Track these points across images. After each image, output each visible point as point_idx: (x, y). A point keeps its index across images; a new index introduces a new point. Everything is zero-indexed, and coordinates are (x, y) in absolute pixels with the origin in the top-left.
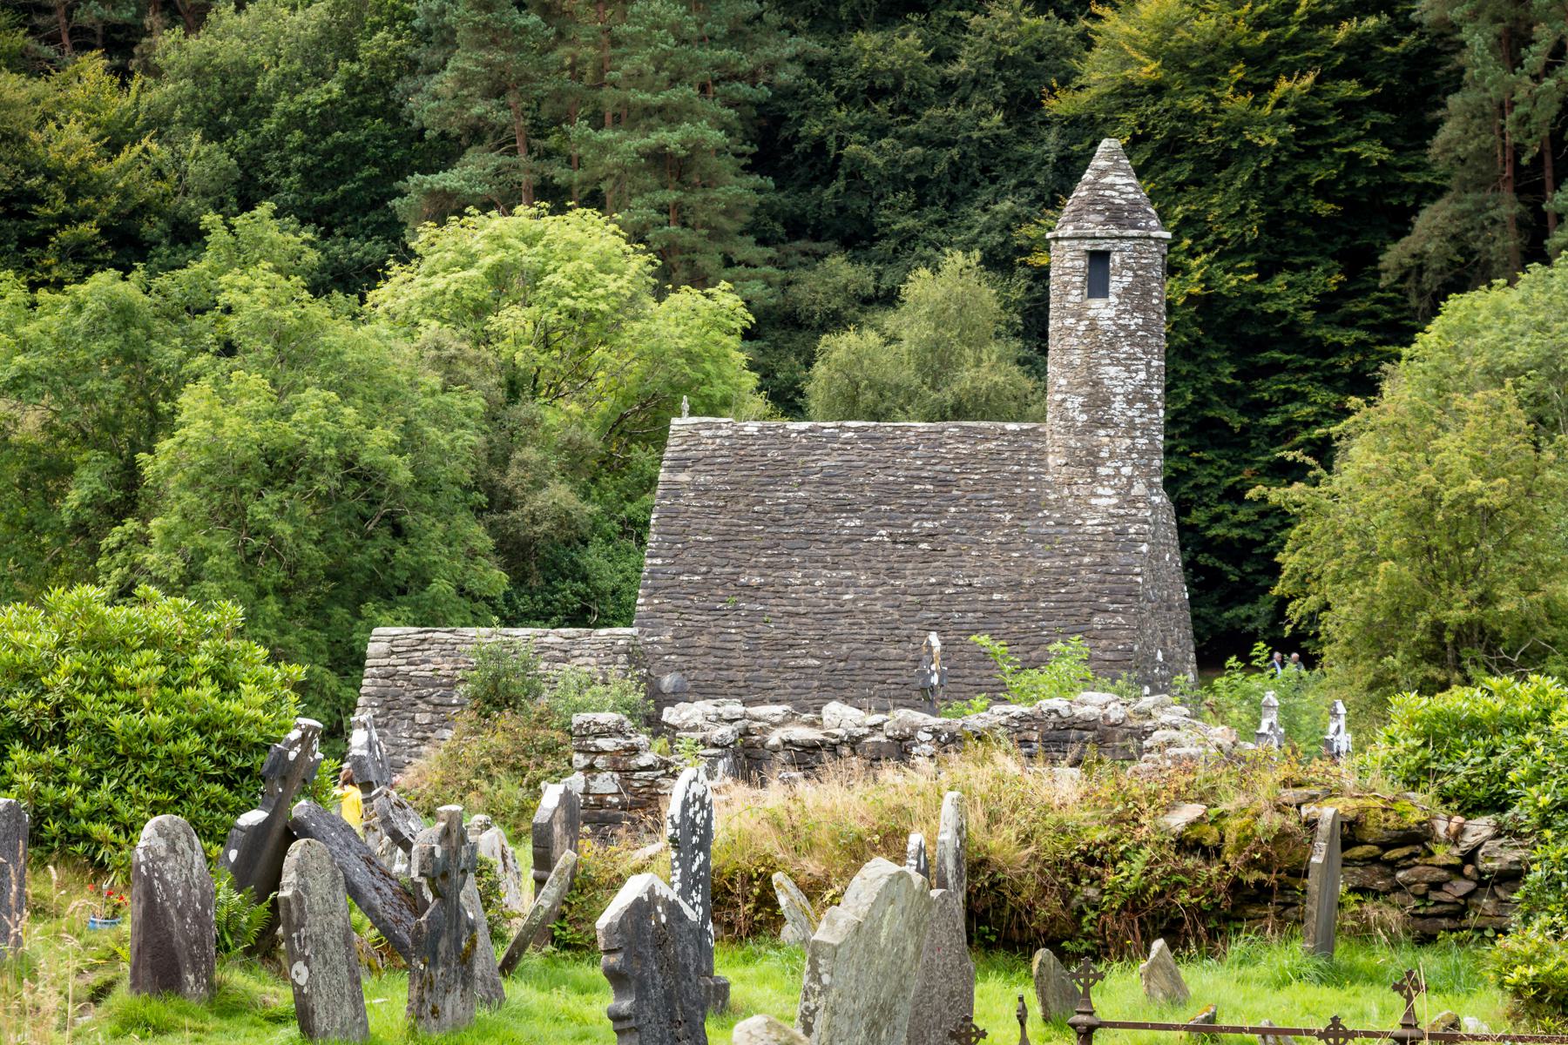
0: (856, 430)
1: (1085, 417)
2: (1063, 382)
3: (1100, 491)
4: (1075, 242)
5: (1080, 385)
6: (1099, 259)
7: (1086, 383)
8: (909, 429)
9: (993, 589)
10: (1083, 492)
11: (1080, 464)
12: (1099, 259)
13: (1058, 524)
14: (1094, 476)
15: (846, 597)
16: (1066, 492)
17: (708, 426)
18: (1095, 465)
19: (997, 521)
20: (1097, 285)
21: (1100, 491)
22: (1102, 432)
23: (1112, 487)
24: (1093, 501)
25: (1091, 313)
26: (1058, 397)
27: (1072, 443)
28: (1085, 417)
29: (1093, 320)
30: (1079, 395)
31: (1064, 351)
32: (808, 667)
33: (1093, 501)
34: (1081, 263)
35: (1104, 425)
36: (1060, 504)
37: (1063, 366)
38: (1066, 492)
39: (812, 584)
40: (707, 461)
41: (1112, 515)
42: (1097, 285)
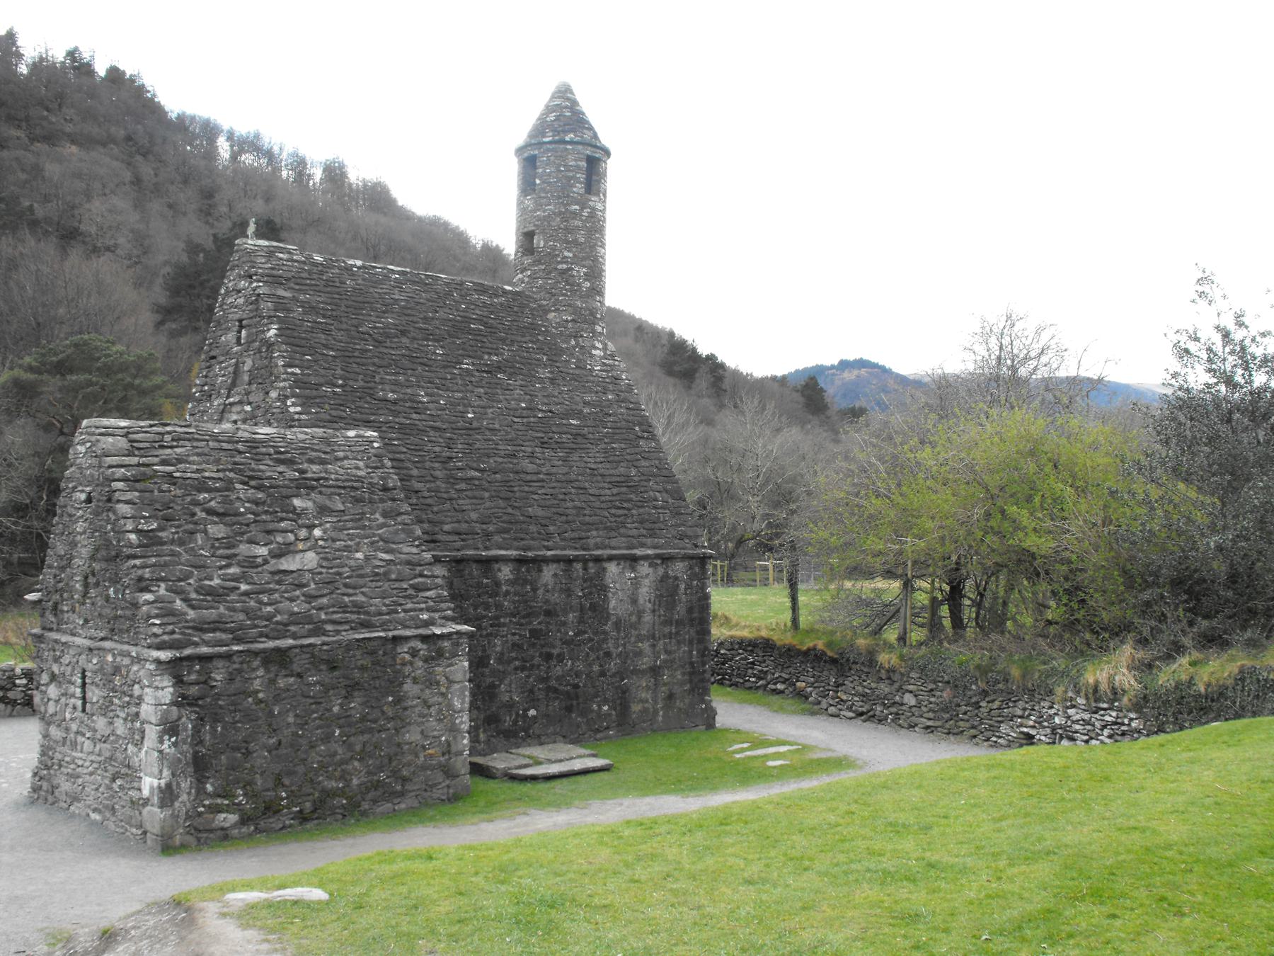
1: (588, 284)
2: (566, 254)
4: (580, 147)
5: (584, 259)
9: (568, 415)
10: (587, 344)
11: (585, 321)
13: (577, 367)
14: (594, 332)
15: (470, 416)
17: (282, 250)
19: (538, 360)
24: (594, 352)
26: (565, 266)
27: (578, 303)
28: (588, 284)
29: (594, 209)
30: (584, 267)
32: (473, 478)
33: (594, 352)
34: (584, 164)
37: (568, 242)
38: (573, 342)
39: (438, 402)
40: (298, 280)
41: (604, 364)
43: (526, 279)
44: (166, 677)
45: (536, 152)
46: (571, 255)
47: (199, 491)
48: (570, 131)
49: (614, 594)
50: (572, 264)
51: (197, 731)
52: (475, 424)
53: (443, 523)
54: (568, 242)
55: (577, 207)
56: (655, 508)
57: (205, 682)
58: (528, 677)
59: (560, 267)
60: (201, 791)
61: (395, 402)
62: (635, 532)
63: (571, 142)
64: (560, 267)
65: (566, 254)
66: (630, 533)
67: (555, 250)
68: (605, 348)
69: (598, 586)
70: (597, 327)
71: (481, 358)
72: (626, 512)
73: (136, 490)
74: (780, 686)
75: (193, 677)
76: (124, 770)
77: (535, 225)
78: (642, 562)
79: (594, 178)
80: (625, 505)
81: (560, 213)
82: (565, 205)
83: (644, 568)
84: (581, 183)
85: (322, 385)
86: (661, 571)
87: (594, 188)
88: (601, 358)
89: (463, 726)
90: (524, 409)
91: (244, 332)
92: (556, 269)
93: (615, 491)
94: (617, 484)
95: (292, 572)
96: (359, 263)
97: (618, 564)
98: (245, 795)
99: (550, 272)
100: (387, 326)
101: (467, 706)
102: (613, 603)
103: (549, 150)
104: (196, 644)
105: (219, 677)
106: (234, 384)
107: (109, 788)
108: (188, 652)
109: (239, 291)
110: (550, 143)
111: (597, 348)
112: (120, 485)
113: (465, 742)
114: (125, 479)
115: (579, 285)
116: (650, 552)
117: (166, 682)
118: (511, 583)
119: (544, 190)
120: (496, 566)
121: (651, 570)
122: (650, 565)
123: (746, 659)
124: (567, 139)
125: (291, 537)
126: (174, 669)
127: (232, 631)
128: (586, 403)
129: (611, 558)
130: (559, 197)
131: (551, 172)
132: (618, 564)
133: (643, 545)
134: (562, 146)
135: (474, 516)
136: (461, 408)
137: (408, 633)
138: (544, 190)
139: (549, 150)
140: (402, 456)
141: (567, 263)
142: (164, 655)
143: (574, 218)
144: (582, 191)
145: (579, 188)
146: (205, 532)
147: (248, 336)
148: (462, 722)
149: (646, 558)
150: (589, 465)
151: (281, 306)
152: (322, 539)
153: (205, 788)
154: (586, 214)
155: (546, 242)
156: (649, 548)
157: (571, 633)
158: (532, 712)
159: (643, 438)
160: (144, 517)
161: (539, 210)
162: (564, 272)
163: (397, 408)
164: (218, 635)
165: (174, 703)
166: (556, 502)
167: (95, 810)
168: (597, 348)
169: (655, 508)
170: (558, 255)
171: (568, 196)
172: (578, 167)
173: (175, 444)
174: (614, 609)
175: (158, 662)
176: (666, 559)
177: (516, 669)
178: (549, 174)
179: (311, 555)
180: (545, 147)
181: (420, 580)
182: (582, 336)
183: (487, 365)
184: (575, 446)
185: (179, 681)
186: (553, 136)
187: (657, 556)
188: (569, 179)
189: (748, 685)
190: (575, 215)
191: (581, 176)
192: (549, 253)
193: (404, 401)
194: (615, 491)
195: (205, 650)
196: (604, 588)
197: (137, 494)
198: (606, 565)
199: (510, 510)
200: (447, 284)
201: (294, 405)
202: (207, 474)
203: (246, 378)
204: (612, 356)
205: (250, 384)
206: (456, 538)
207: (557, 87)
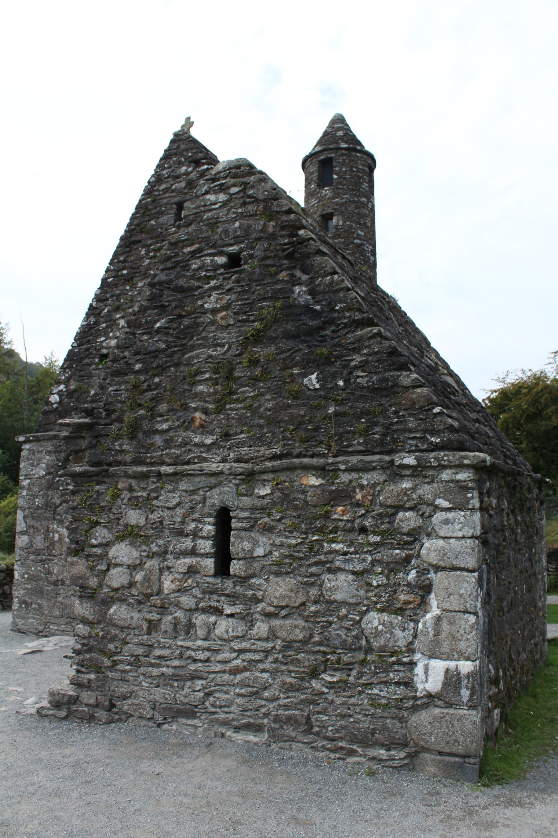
2: (360, 232)
4: (365, 157)
34: (366, 169)
37: (360, 224)
45: (333, 155)
46: (363, 234)
50: (364, 241)
54: (360, 224)
59: (356, 241)
64: (356, 241)
65: (360, 232)
77: (333, 209)
81: (354, 202)
92: (353, 243)
99: (349, 245)
103: (343, 155)
115: (368, 257)
130: (353, 190)
131: (346, 171)
134: (354, 153)
141: (360, 239)
143: (363, 208)
155: (344, 222)
161: (337, 198)
170: (354, 233)
171: (359, 190)
178: (345, 172)
180: (340, 152)
188: (359, 178)
192: (347, 230)
207: (335, 117)
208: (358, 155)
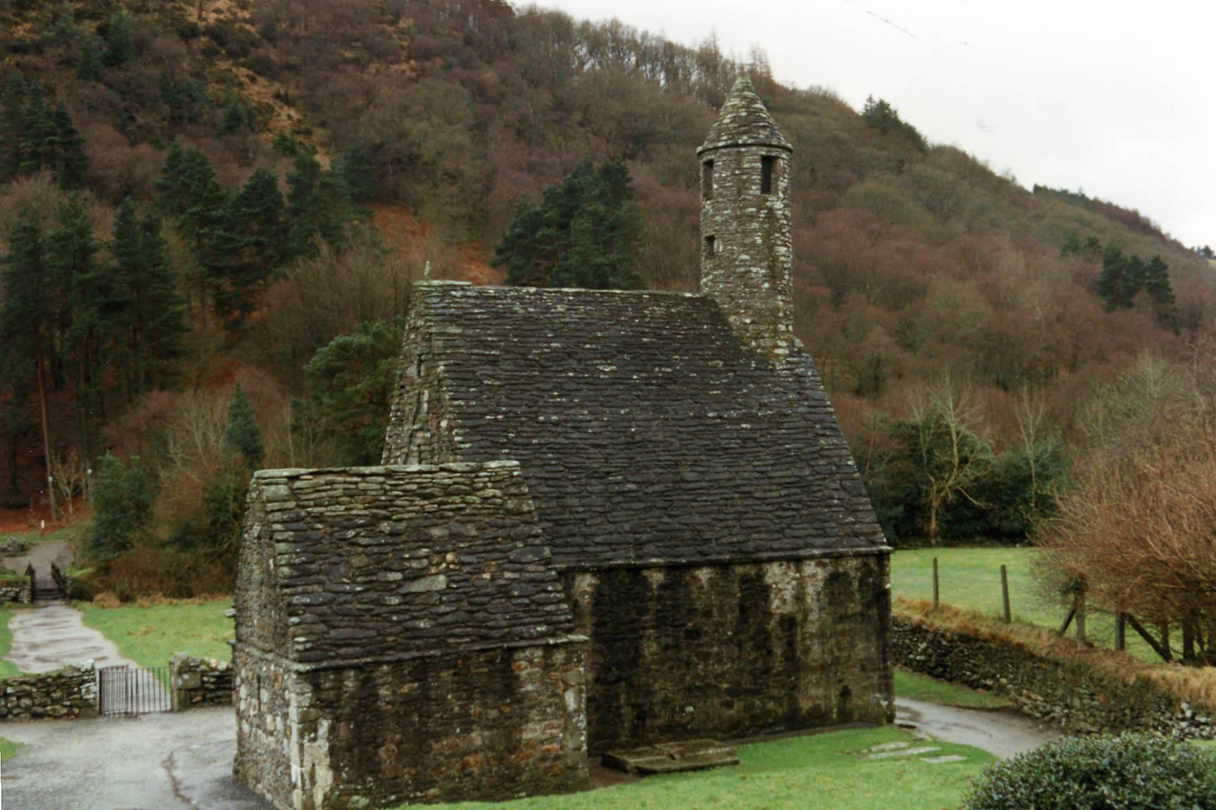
0: (575, 294)
1: (766, 285)
2: (744, 257)
3: (780, 343)
4: (754, 148)
5: (761, 261)
6: (768, 162)
7: (767, 258)
8: (613, 295)
10: (768, 343)
12: (768, 162)
14: (776, 331)
16: (754, 344)
17: (454, 288)
18: (775, 323)
19: (714, 367)
20: (767, 187)
21: (780, 343)
22: (779, 297)
23: (785, 340)
25: (768, 204)
26: (742, 269)
28: (766, 285)
29: (771, 210)
31: (745, 233)
32: (630, 491)
34: (759, 165)
35: (780, 292)
36: (751, 354)
41: (788, 362)
42: (767, 187)
43: (710, 284)
44: (305, 684)
45: (713, 157)
47: (348, 528)
48: (745, 133)
49: (776, 594)
50: (750, 266)
51: (332, 730)
52: (638, 438)
53: (594, 535)
54: (745, 245)
55: (754, 210)
56: (829, 506)
57: (338, 686)
58: (684, 675)
60: (337, 778)
61: (556, 424)
62: (803, 533)
63: (744, 145)
65: (744, 257)
66: (797, 533)
67: (733, 254)
68: (791, 344)
69: (758, 591)
70: (780, 326)
71: (652, 371)
72: (794, 513)
73: (292, 530)
74: (989, 682)
75: (327, 685)
76: (282, 760)
78: (808, 562)
79: (773, 176)
80: (794, 506)
81: (737, 217)
82: (741, 209)
83: (810, 568)
84: (756, 184)
85: (486, 414)
86: (830, 569)
87: (773, 187)
88: (786, 356)
89: (579, 724)
90: (691, 418)
91: (423, 368)
92: (735, 273)
93: (783, 492)
94: (788, 485)
95: (422, 593)
96: (533, 290)
97: (781, 565)
98: (374, 782)
99: (729, 276)
100: (555, 350)
101: (583, 706)
102: (776, 603)
103: (724, 154)
104: (332, 658)
105: (350, 684)
106: (418, 412)
107: (275, 773)
108: (325, 664)
109: (418, 328)
110: (724, 147)
111: (781, 347)
112: (278, 527)
113: (583, 738)
114: (283, 522)
116: (816, 552)
117: (307, 688)
118: (662, 587)
119: (720, 195)
120: (645, 573)
121: (819, 570)
122: (818, 565)
123: (962, 652)
124: (740, 142)
125: (425, 562)
126: (312, 678)
127: (362, 646)
128: (762, 406)
129: (770, 560)
132: (781, 565)
133: (807, 546)
134: (736, 149)
135: (627, 527)
136: (626, 424)
137: (523, 643)
138: (720, 195)
139: (724, 154)
140: (559, 475)
142: (302, 667)
143: (751, 221)
144: (758, 192)
145: (755, 190)
146: (347, 563)
147: (427, 369)
148: (578, 721)
149: (812, 557)
150: (758, 469)
151: (450, 343)
152: (453, 563)
153: (340, 775)
154: (763, 215)
155: (725, 246)
156: (816, 547)
157: (730, 633)
158: (690, 709)
159: (823, 435)
160: (297, 553)
162: (742, 275)
163: (560, 429)
164: (351, 650)
165: (311, 706)
166: (716, 508)
167: (269, 791)
168: (781, 347)
169: (829, 506)
172: (753, 168)
173: (329, 487)
174: (778, 608)
175: (298, 673)
176: (840, 557)
177: (671, 668)
178: (725, 179)
179: (442, 578)
181: (543, 595)
182: (763, 337)
183: (657, 378)
184: (743, 450)
185: (317, 688)
186: (729, 139)
187: (825, 556)
188: (744, 182)
189: (964, 678)
190: (752, 217)
191: (757, 177)
192: (728, 258)
193: (566, 421)
194: (783, 492)
195: (339, 662)
196: (766, 590)
197: (292, 533)
198: (766, 567)
199: (666, 519)
200: (622, 300)
201: (457, 434)
202: (354, 512)
203: (425, 405)
204: (799, 353)
205: (428, 413)
206: (606, 548)
208: (743, 149)
